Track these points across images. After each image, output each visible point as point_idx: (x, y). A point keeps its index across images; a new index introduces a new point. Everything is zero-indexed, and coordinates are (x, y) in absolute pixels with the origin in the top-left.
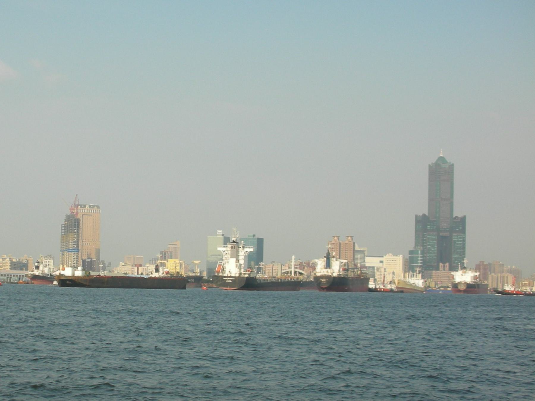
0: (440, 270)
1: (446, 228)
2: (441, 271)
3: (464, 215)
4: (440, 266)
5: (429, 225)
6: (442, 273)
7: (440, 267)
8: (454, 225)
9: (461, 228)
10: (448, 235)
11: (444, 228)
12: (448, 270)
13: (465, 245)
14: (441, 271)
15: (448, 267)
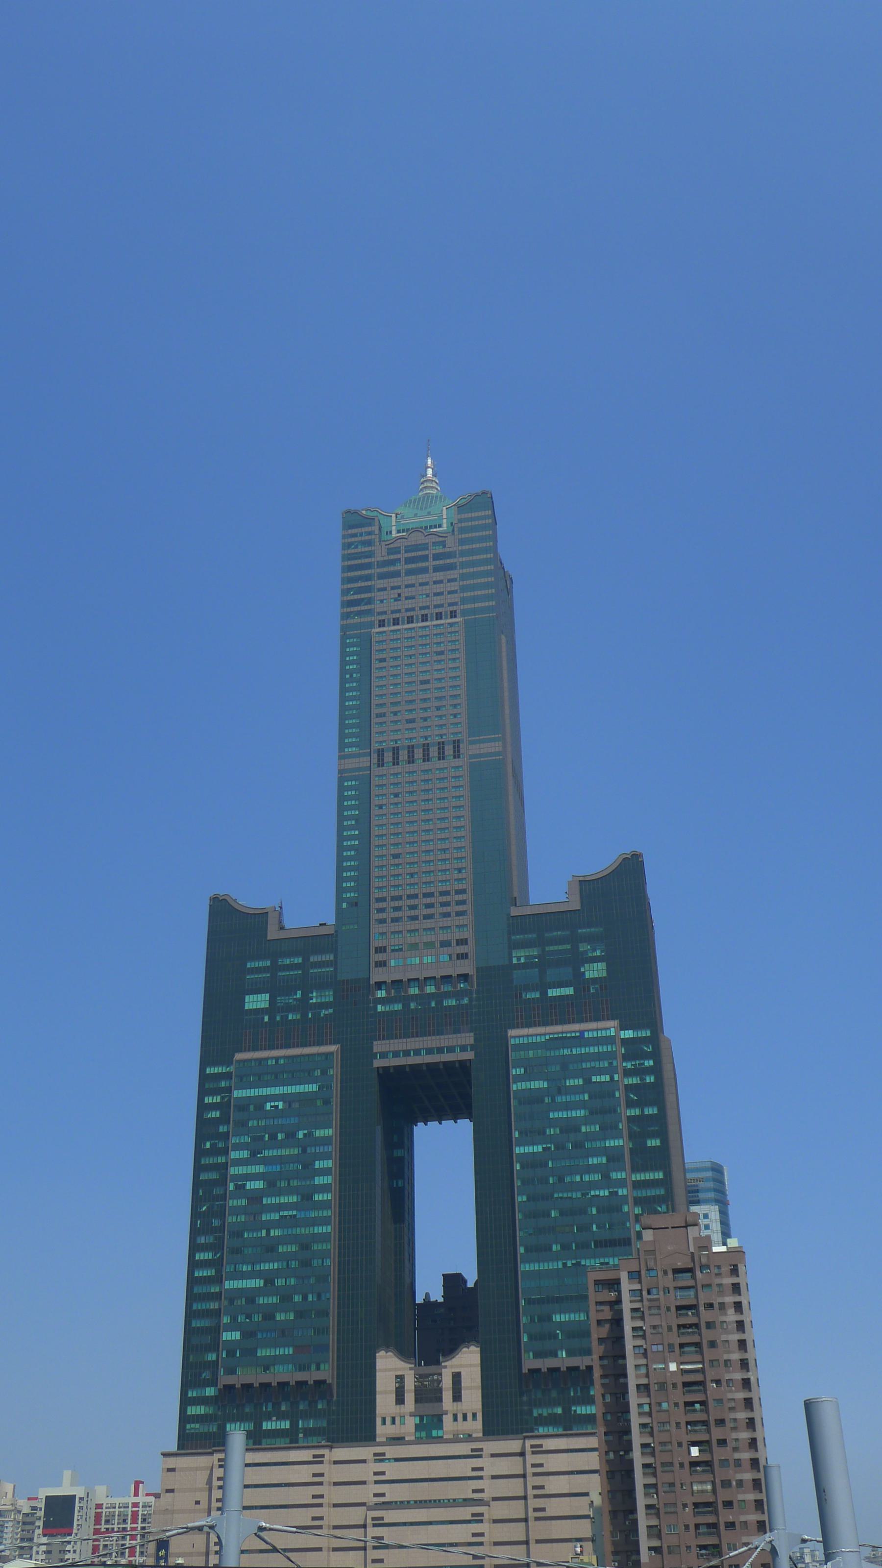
0: (382, 1431)
1: (430, 989)
2: (397, 1440)
3: (627, 849)
4: (384, 1383)
5: (256, 990)
6: (392, 1470)
7: (385, 1403)
8: (520, 956)
9: (595, 971)
10: (469, 1055)
11: (414, 991)
12: (478, 1425)
13: (663, 1134)
14: (397, 1440)
15: (473, 1399)
